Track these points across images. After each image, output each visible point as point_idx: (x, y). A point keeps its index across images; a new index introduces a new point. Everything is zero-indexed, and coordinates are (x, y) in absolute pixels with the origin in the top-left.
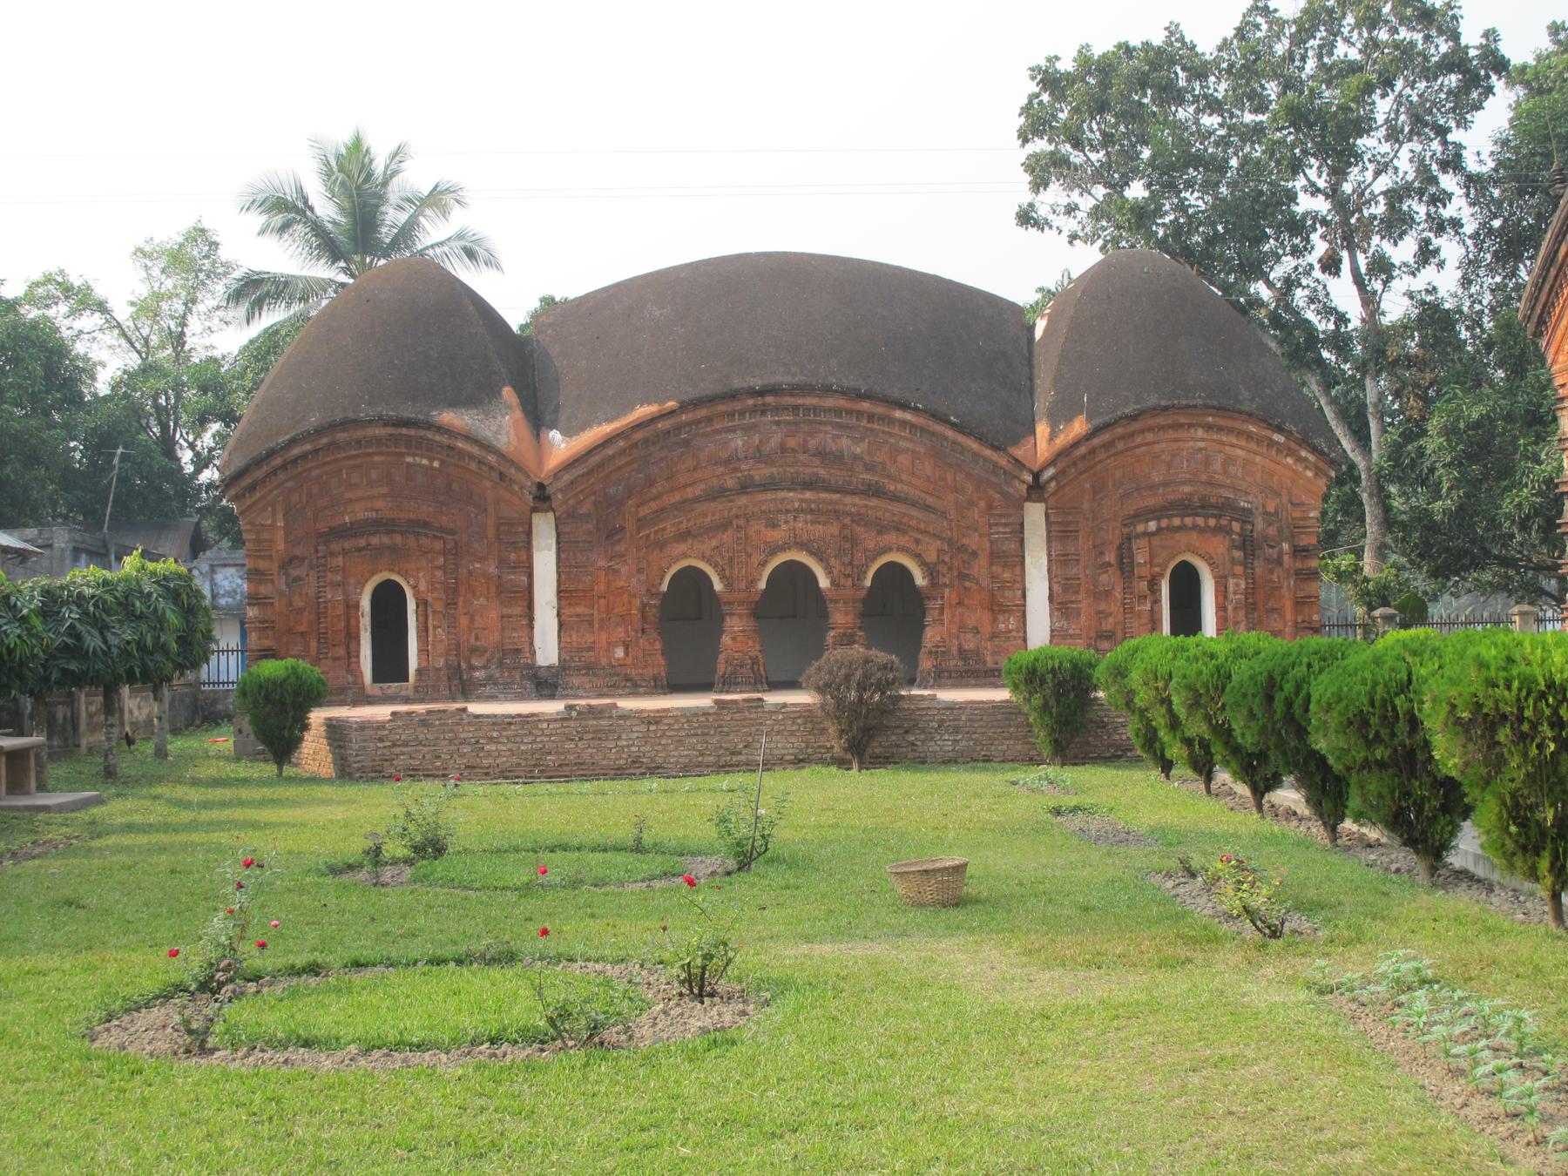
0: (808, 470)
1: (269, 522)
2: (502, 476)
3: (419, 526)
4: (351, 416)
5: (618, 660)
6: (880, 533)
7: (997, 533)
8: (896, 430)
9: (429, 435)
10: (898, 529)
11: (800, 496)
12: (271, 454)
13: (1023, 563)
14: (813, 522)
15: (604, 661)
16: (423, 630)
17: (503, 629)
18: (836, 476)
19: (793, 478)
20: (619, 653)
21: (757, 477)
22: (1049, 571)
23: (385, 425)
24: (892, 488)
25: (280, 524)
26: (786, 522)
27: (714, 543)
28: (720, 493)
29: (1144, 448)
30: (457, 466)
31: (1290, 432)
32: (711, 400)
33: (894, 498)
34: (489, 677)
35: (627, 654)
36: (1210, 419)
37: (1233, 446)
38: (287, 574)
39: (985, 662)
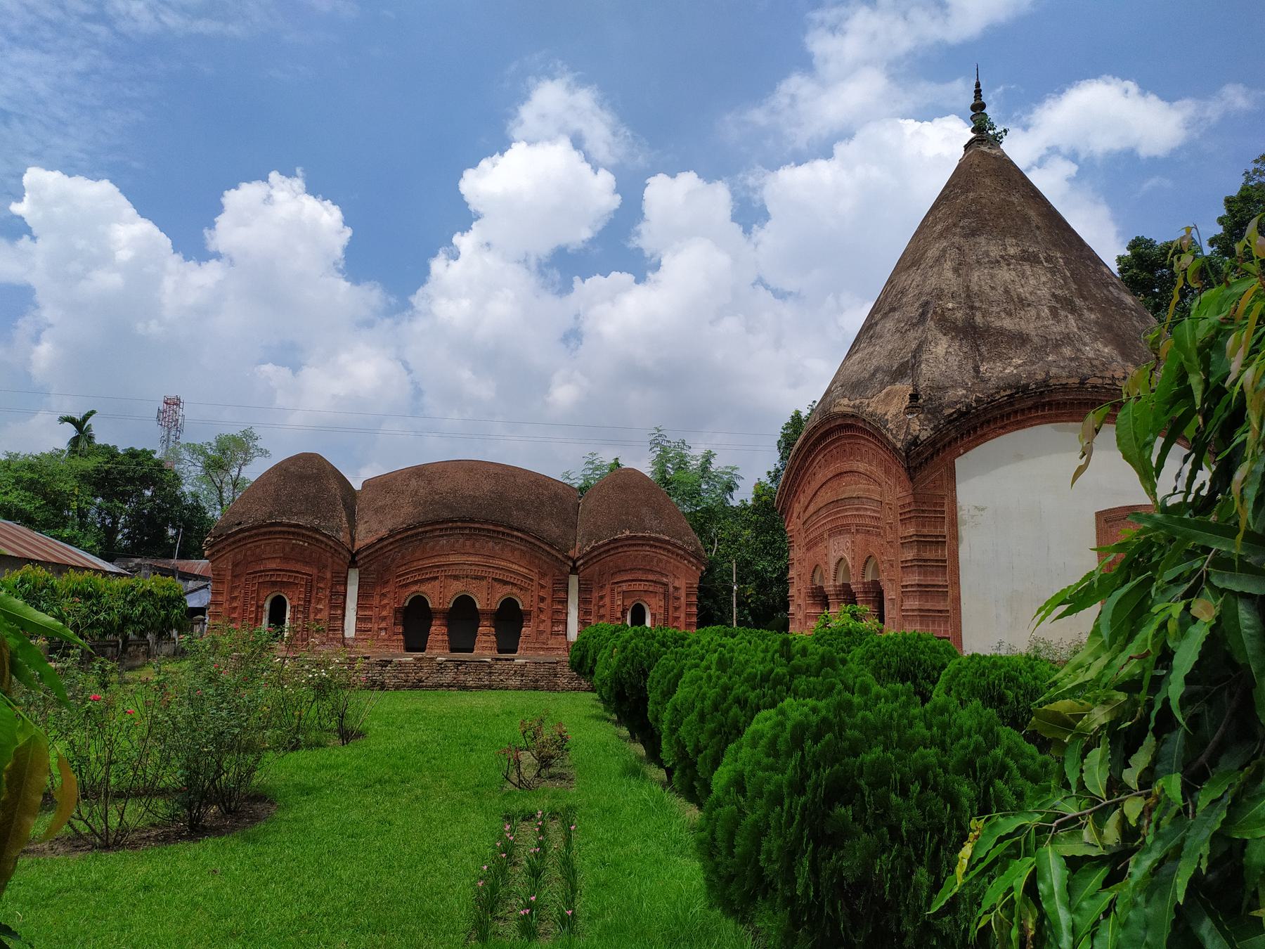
2: (336, 550)
8: (514, 540)
16: (293, 619)
32: (433, 523)
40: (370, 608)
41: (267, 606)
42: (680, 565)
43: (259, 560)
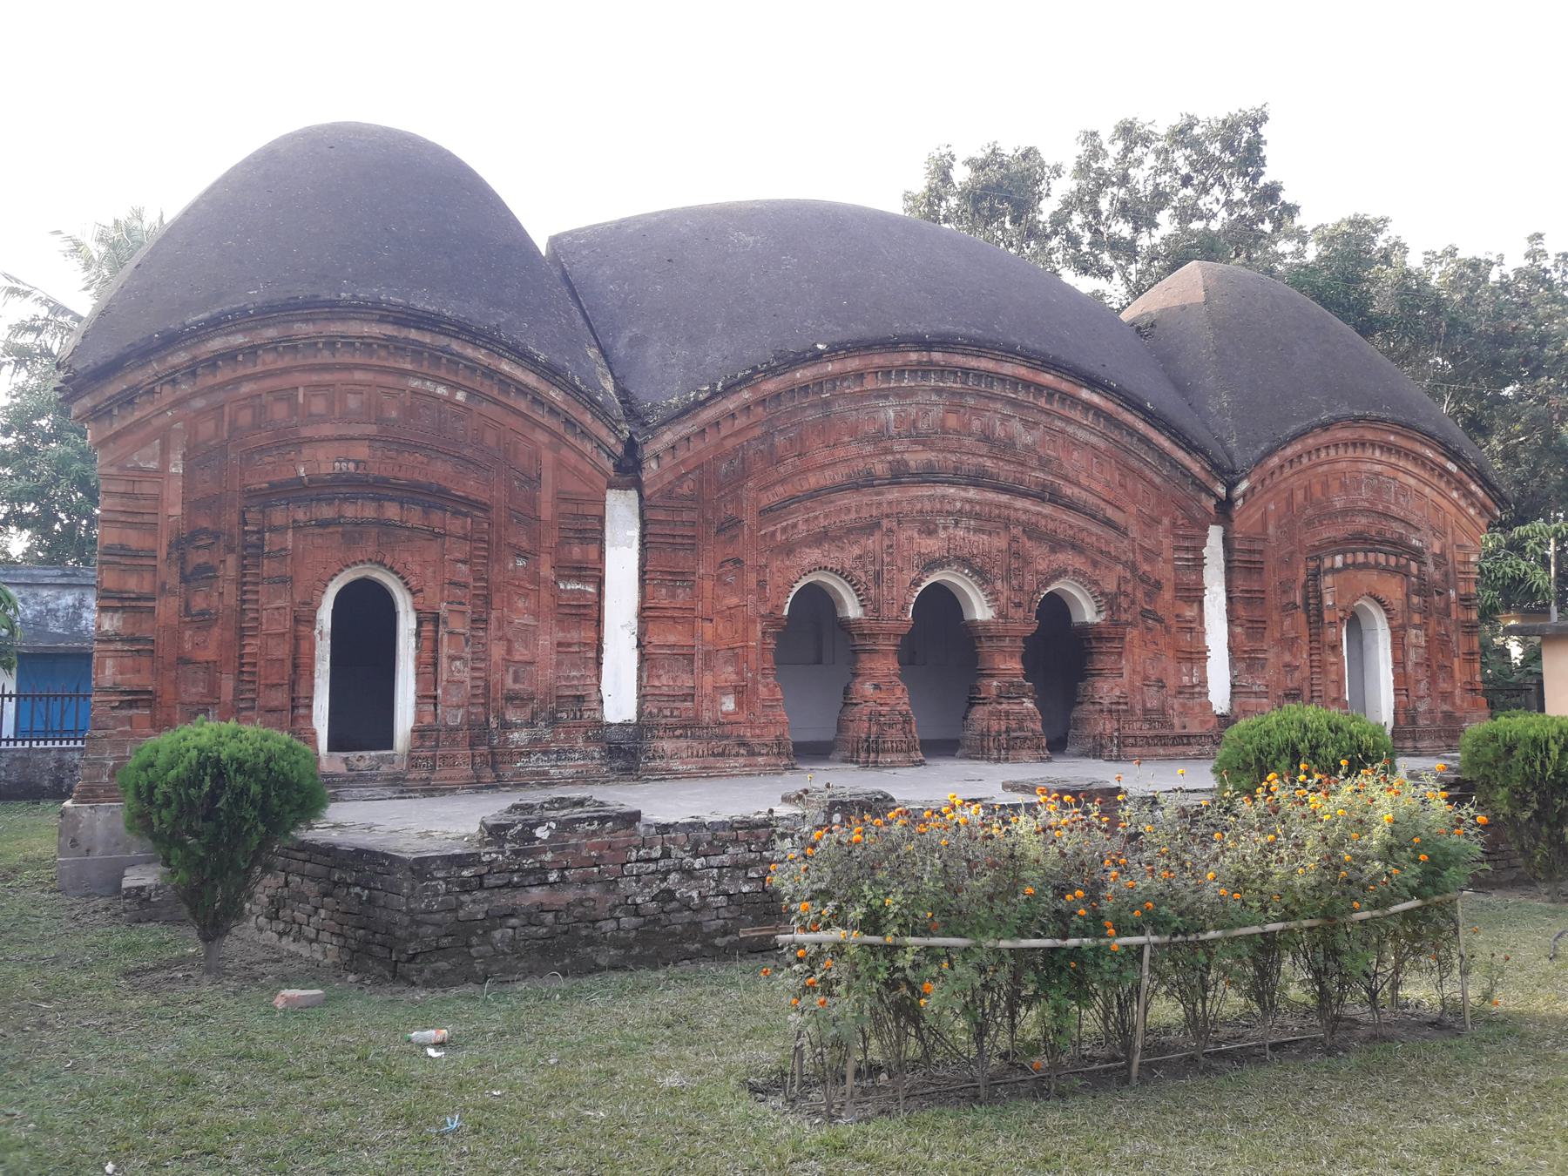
0: (973, 460)
1: (153, 465)
3: (432, 497)
4: (326, 295)
5: (727, 714)
6: (1053, 550)
7: (1180, 559)
8: (1076, 415)
9: (456, 346)
10: (1074, 547)
11: (963, 494)
12: (171, 341)
13: (1201, 603)
14: (977, 530)
15: (707, 716)
16: (428, 668)
17: (559, 664)
18: (1005, 470)
19: (956, 469)
20: (729, 704)
21: (912, 463)
22: (1230, 612)
23: (382, 320)
24: (1069, 492)
25: (176, 469)
26: (945, 528)
27: (856, 551)
28: (866, 482)
29: (1325, 468)
30: (496, 402)
31: (1467, 461)
33: (1071, 506)
34: (535, 741)
35: (739, 704)
36: (1392, 438)
37: (1407, 472)
38: (183, 559)
39: (1172, 726)
40: (686, 618)
41: (325, 616)
42: (1444, 503)
43: (286, 442)
